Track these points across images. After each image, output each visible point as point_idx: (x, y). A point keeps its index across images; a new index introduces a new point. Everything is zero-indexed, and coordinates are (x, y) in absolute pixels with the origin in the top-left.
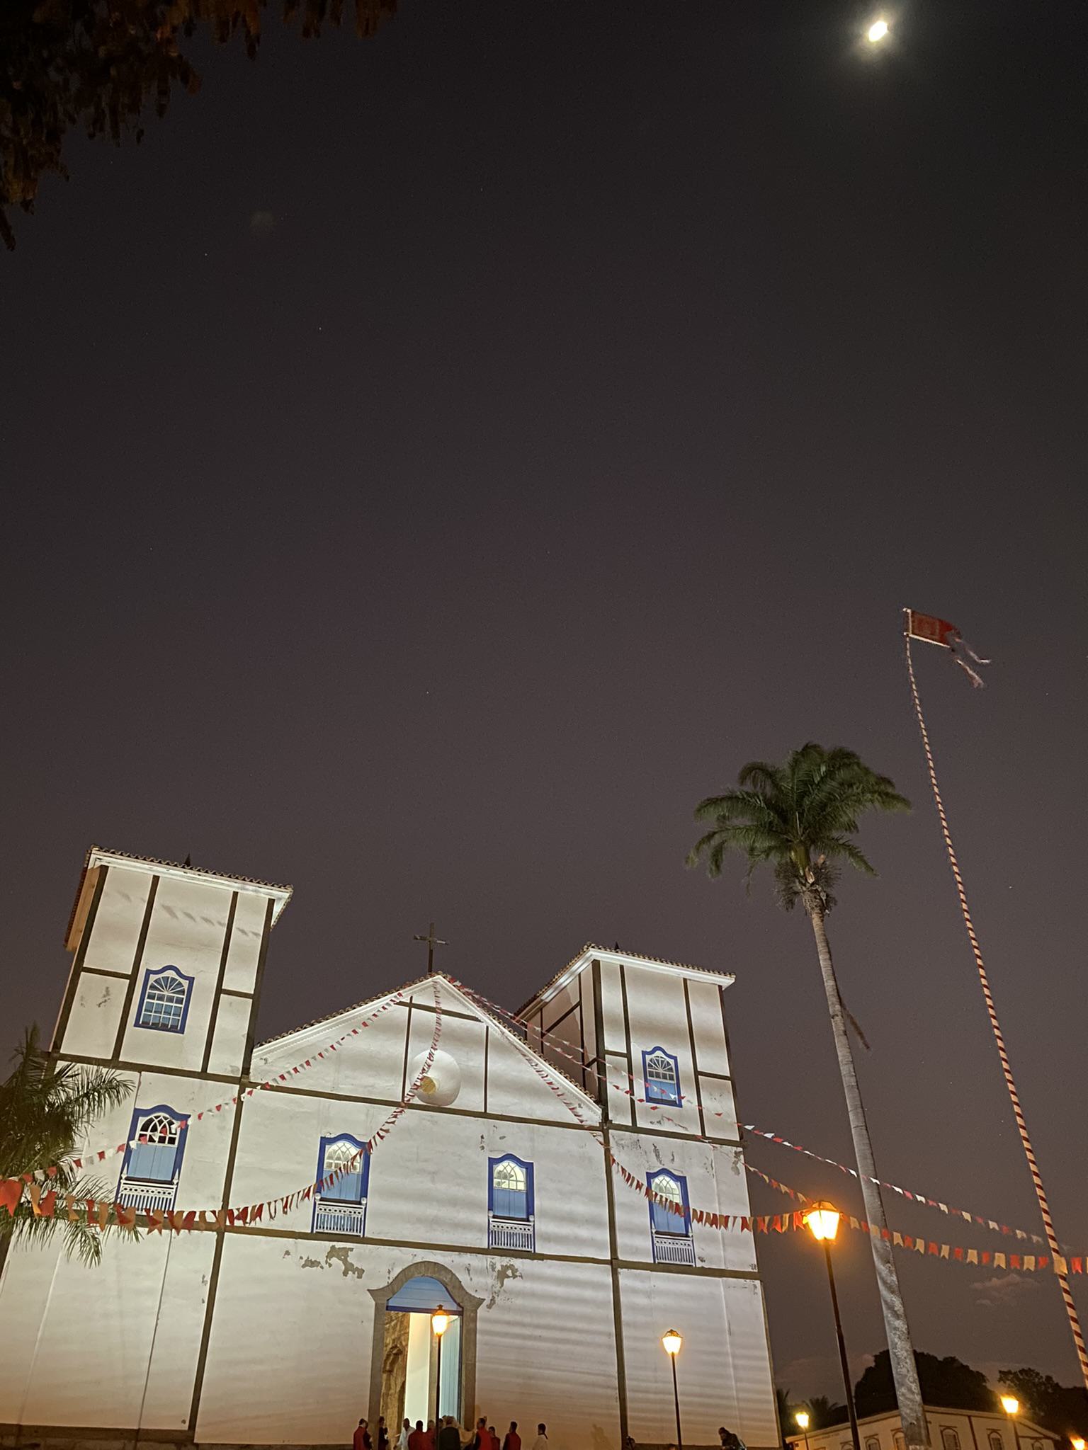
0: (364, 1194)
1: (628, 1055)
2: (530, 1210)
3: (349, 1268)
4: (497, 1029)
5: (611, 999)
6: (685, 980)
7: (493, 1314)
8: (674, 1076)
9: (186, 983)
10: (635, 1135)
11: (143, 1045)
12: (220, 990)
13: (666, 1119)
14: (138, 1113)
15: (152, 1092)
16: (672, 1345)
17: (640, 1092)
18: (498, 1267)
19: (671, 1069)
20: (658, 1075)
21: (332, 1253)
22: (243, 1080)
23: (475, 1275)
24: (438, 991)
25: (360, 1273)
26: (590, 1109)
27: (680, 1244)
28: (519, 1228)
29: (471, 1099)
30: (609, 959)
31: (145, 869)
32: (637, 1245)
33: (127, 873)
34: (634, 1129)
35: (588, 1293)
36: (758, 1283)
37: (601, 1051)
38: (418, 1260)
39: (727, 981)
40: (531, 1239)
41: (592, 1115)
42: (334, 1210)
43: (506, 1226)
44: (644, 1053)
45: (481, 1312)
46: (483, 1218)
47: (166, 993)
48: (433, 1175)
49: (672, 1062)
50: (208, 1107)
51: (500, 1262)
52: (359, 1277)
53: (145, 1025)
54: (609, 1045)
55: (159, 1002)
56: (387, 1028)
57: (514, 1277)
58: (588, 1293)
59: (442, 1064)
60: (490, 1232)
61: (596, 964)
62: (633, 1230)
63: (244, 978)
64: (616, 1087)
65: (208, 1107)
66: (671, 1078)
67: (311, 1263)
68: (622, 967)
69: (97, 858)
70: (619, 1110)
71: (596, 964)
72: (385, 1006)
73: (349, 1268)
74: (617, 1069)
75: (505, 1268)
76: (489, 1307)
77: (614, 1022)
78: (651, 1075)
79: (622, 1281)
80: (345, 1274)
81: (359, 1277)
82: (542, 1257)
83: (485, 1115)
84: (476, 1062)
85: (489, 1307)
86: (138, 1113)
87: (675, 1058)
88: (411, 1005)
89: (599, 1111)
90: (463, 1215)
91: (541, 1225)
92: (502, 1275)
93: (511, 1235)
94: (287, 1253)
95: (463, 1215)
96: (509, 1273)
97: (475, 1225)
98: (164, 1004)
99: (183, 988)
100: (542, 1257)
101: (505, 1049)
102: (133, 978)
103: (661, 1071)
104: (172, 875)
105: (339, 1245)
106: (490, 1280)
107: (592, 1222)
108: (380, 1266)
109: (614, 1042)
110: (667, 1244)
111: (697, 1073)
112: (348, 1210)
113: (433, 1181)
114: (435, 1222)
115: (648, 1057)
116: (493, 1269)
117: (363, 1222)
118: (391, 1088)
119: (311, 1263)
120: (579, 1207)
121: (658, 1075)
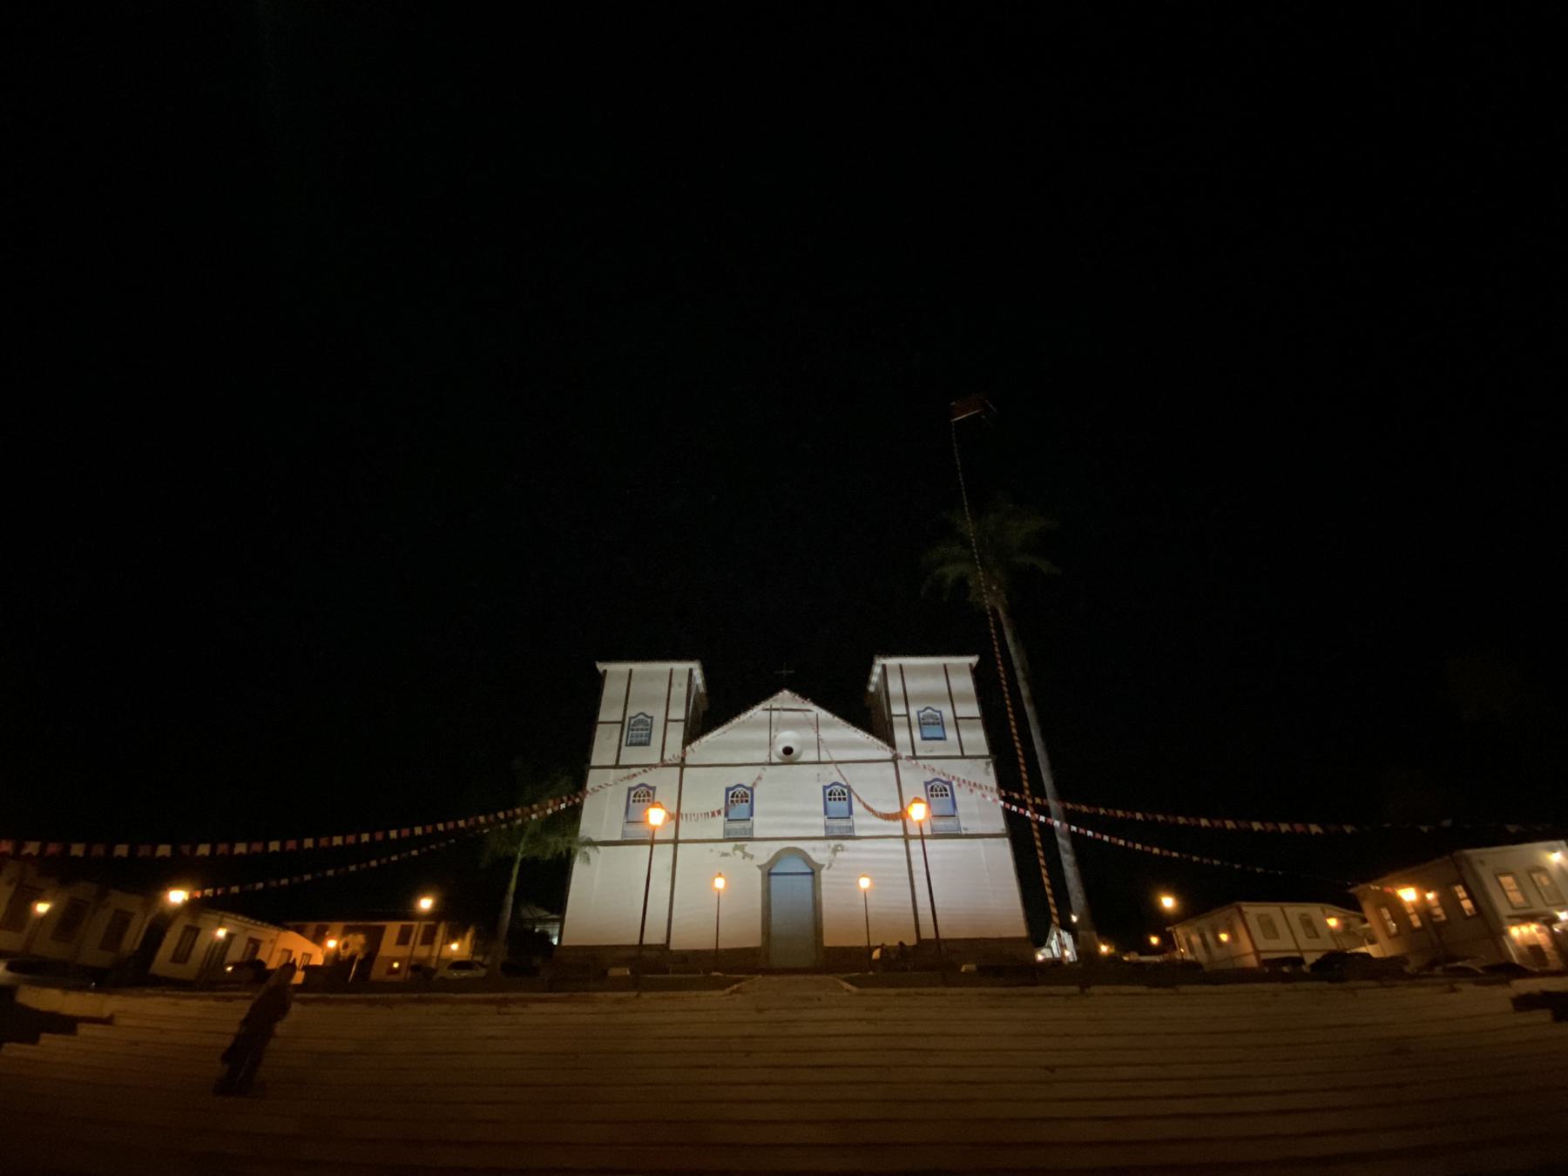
1: (908, 715)
2: (851, 812)
3: (745, 855)
4: (824, 715)
5: (895, 686)
7: (831, 872)
8: (941, 723)
11: (631, 755)
12: (667, 720)
13: (938, 748)
14: (630, 789)
16: (720, 883)
17: (917, 735)
21: (736, 848)
22: (682, 765)
23: (819, 852)
24: (785, 697)
25: (752, 857)
28: (844, 823)
29: (813, 756)
30: (892, 662)
31: (621, 668)
33: (615, 671)
34: (914, 757)
35: (891, 856)
37: (891, 716)
39: (974, 660)
40: (852, 828)
41: (887, 753)
42: (736, 825)
45: (824, 872)
46: (821, 820)
51: (833, 843)
53: (631, 744)
55: (637, 732)
56: (757, 725)
58: (891, 856)
59: (787, 737)
60: (826, 827)
61: (884, 667)
63: (679, 712)
64: (901, 735)
65: (664, 781)
69: (601, 667)
71: (884, 667)
72: (758, 712)
73: (745, 855)
74: (901, 724)
83: (819, 763)
84: (810, 735)
86: (630, 789)
88: (771, 710)
90: (808, 821)
92: (835, 851)
95: (808, 821)
97: (817, 824)
98: (641, 734)
99: (646, 723)
101: (828, 725)
102: (623, 723)
104: (638, 667)
106: (828, 854)
109: (897, 709)
112: (743, 824)
114: (792, 826)
117: (751, 829)
118: (762, 756)
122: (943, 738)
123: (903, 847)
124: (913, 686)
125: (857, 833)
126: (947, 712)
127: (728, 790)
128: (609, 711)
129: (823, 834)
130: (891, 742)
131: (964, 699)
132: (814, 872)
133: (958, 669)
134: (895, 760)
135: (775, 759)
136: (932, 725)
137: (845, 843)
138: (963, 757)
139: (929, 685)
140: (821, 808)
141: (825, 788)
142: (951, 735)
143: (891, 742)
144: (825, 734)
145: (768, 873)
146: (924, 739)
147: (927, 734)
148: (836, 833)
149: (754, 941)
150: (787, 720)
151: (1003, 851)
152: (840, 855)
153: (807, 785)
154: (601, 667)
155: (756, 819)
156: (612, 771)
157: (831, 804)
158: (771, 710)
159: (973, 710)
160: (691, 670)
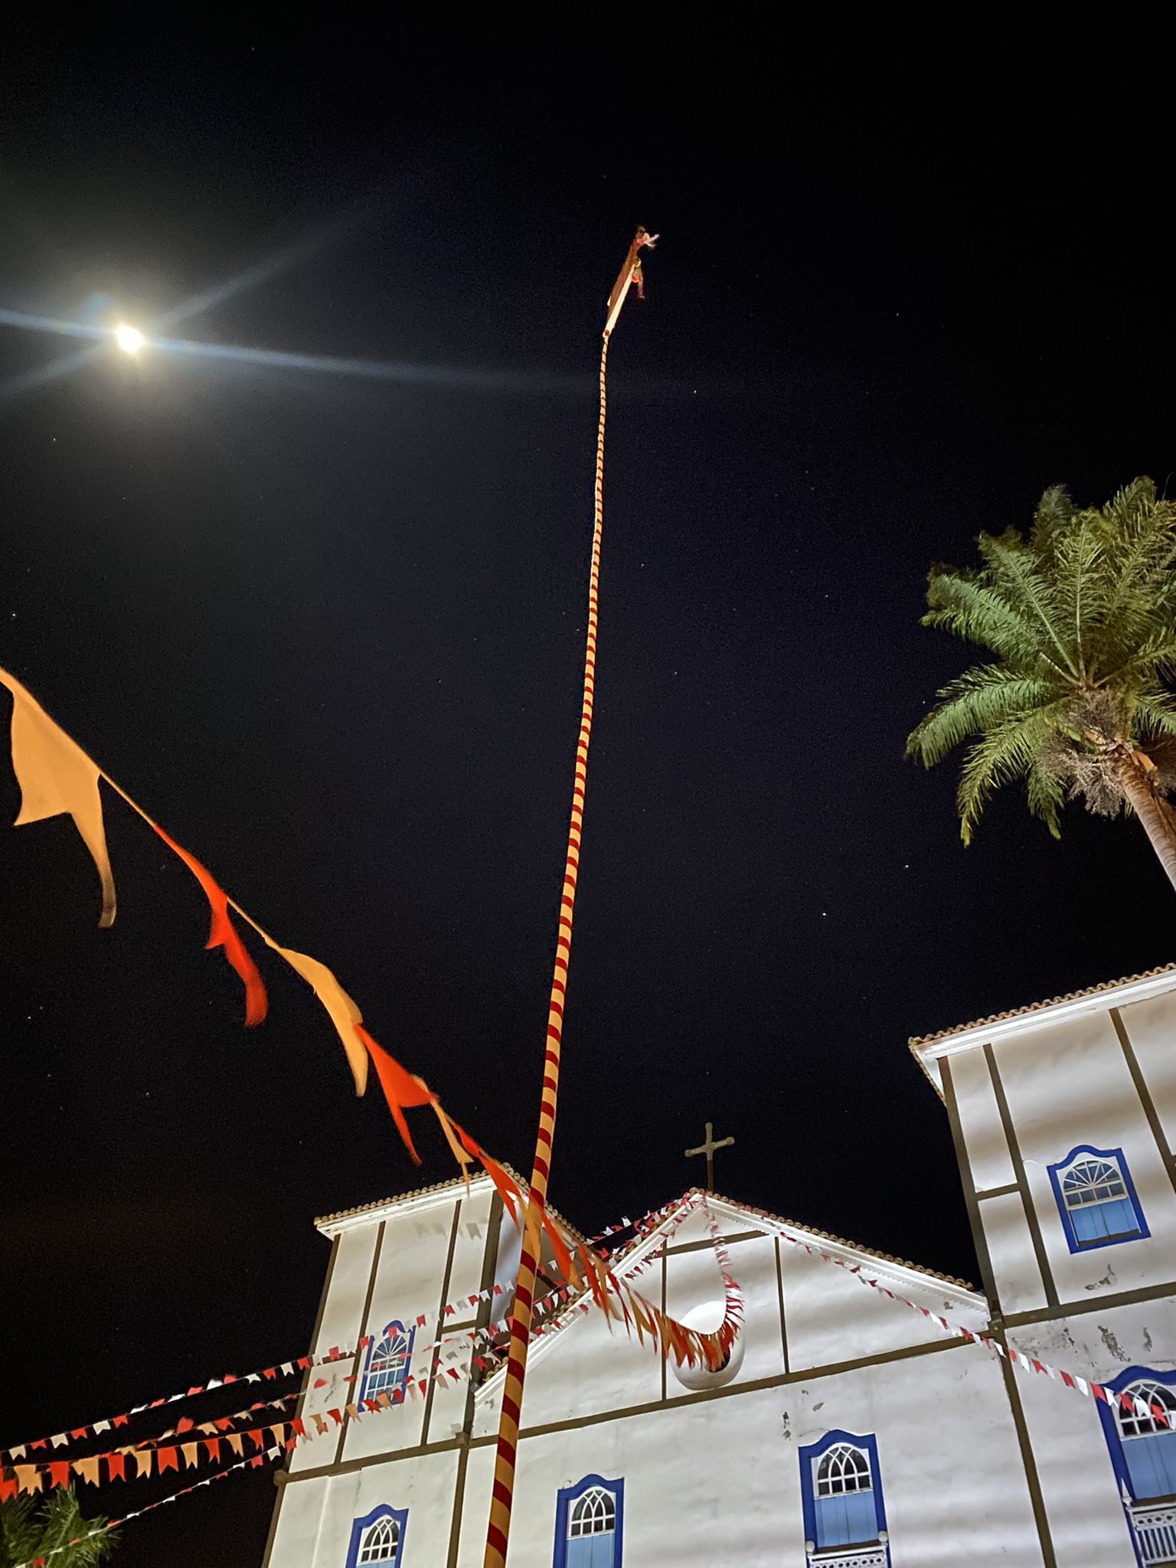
1: (1022, 1186)
2: (882, 1526)
10: (1058, 1324)
12: (441, 1330)
15: (376, 1488)
17: (1055, 1240)
19: (1114, 1175)
20: (1087, 1197)
24: (700, 1212)
26: (972, 1306)
34: (1056, 1310)
41: (973, 1312)
44: (1052, 1170)
47: (388, 1358)
48: (714, 1505)
49: (1112, 1161)
50: (423, 1490)
54: (982, 1181)
62: (1078, 1514)
64: (1006, 1252)
66: (1117, 1190)
68: (988, 1048)
69: (326, 1227)
70: (1019, 1288)
74: (1005, 1219)
77: (986, 1145)
78: (1073, 1200)
83: (788, 1378)
87: (1118, 1153)
89: (982, 1302)
101: (809, 1261)
103: (1092, 1186)
104: (393, 1212)
107: (994, 1517)
109: (987, 1176)
113: (715, 1515)
115: (1061, 1175)
120: (969, 1496)
121: (1087, 1197)
124: (1025, 1096)
128: (335, 1333)
134: (998, 1327)
140: (798, 1518)
141: (806, 1455)
144: (804, 1293)
147: (1086, 1234)
154: (326, 1227)
156: (329, 1480)
158: (664, 1253)
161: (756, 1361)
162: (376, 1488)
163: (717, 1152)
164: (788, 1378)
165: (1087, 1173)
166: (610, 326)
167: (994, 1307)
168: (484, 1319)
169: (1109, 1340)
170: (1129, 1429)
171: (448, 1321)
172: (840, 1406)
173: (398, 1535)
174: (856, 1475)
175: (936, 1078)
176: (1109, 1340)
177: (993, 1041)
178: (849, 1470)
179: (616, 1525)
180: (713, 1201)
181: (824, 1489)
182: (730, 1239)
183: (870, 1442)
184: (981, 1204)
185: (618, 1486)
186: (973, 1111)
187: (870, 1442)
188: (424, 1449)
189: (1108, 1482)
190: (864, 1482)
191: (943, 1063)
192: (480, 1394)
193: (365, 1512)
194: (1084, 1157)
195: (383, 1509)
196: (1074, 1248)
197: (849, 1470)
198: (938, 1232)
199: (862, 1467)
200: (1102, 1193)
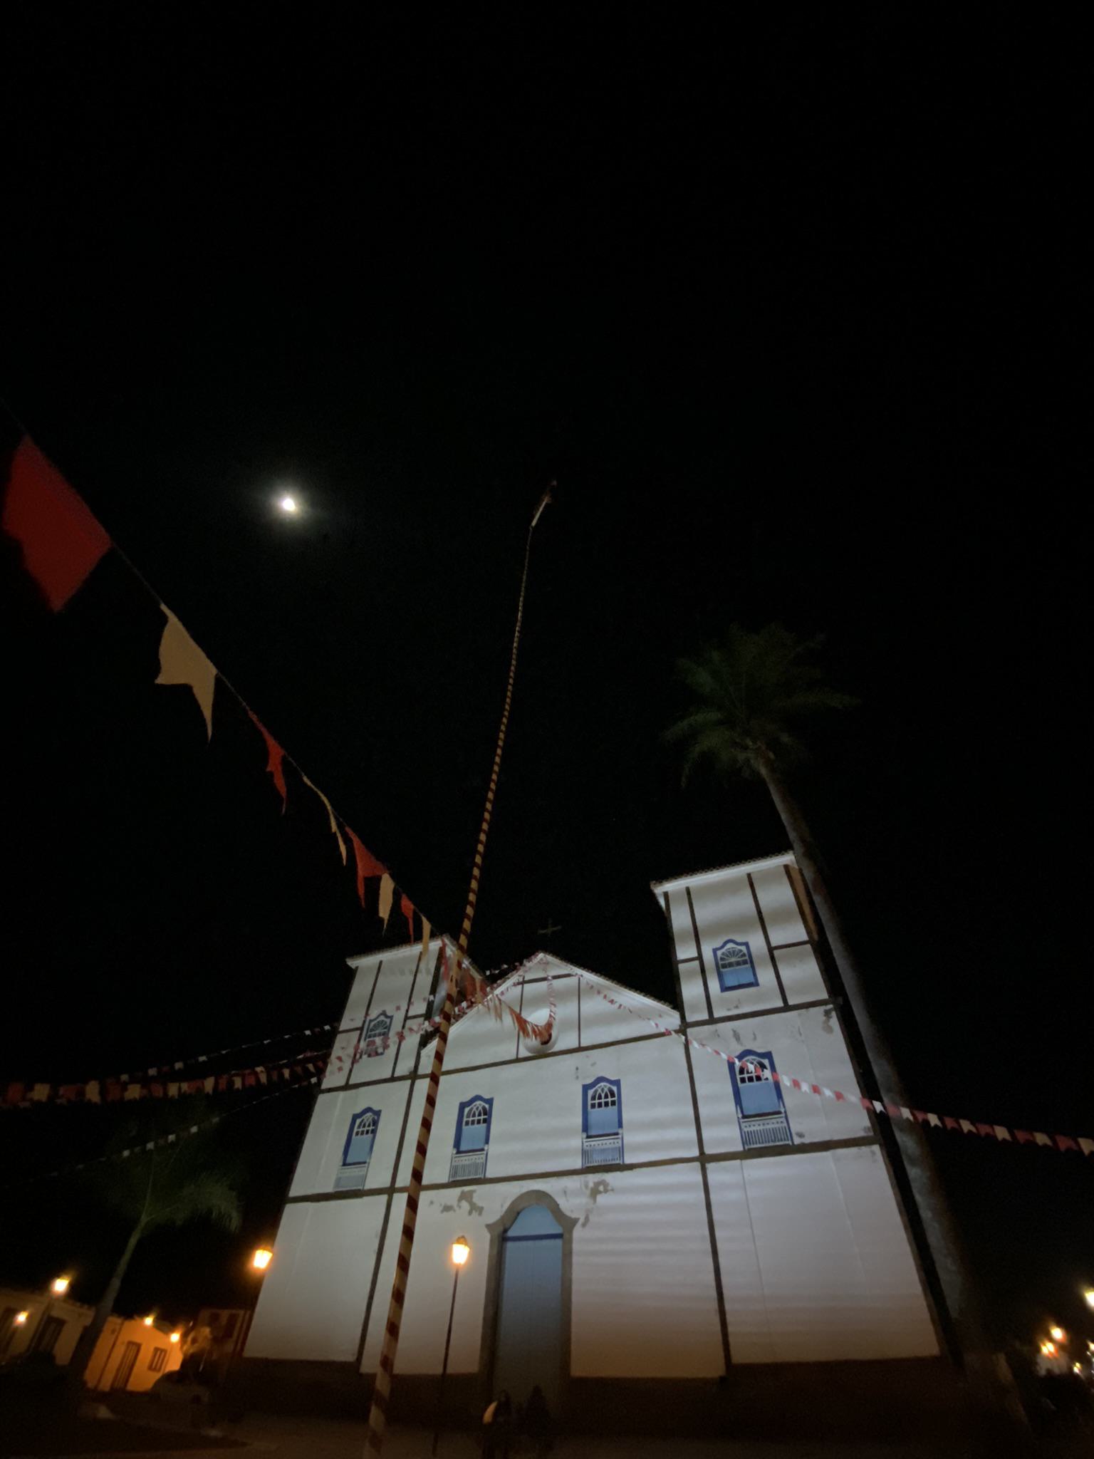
0: (487, 1142)
1: (700, 957)
2: (620, 1125)
6: (749, 875)
9: (388, 1021)
12: (407, 1018)
13: (746, 1001)
17: (714, 985)
18: (591, 1185)
20: (731, 965)
21: (463, 1196)
23: (570, 1196)
24: (542, 964)
25: (480, 1210)
27: (773, 1124)
30: (673, 886)
32: (724, 1133)
34: (712, 1020)
36: (876, 1148)
38: (524, 1190)
41: (671, 1020)
43: (596, 1143)
44: (715, 951)
45: (578, 1233)
46: (577, 1141)
49: (743, 948)
50: (390, 1101)
51: (592, 1179)
52: (480, 1214)
57: (606, 1191)
60: (585, 1153)
61: (666, 895)
62: (718, 1121)
64: (691, 990)
66: (745, 962)
67: (447, 1208)
68: (688, 890)
69: (352, 963)
74: (690, 974)
75: (597, 1184)
76: (584, 1225)
78: (724, 966)
79: (711, 1178)
80: (470, 1213)
81: (480, 1214)
82: (631, 1167)
83: (580, 1049)
85: (584, 1225)
87: (746, 944)
91: (629, 1137)
92: (595, 1193)
93: (603, 1151)
94: (432, 1203)
96: (601, 1188)
100: (631, 1167)
103: (733, 960)
104: (386, 956)
105: (467, 1189)
106: (584, 1200)
108: (496, 1200)
109: (684, 951)
110: (756, 1126)
111: (771, 950)
115: (719, 953)
116: (587, 1186)
119: (447, 1208)
121: (731, 965)
122: (755, 984)
123: (700, 1178)
124: (705, 913)
125: (629, 1160)
126: (757, 942)
127: (586, 1088)
128: (352, 1018)
129: (577, 1164)
130: (675, 1001)
131: (782, 916)
132: (564, 1230)
133: (768, 876)
134: (684, 1027)
135: (524, 1053)
136: (735, 968)
137: (610, 1177)
138: (787, 1008)
139: (734, 906)
140: (579, 1121)
142: (766, 976)
143: (675, 1001)
144: (592, 1006)
145: (502, 1237)
146: (724, 989)
147: (730, 982)
148: (597, 1160)
149: (466, 1358)
150: (558, 993)
151: (870, 1167)
152: (600, 1198)
153: (562, 1081)
154: (352, 963)
155: (492, 1148)
157: (595, 1114)
158: (523, 983)
159: (797, 932)
160: (442, 951)
161: (564, 1040)
162: (364, 1099)
163: (553, 932)
164: (580, 1049)
165: (732, 953)
166: (534, 523)
167: (683, 1017)
168: (428, 1016)
169: (737, 1036)
170: (743, 1080)
171: (410, 1014)
172: (604, 1065)
173: (375, 1123)
174: (610, 1100)
175: (662, 902)
176: (737, 1036)
177: (690, 885)
178: (606, 1097)
179: (487, 1121)
180: (550, 958)
181: (593, 1106)
182: (555, 977)
183: (617, 1083)
184: (681, 967)
185: (490, 1102)
186: (680, 920)
187: (617, 1083)
188: (393, 1079)
189: (731, 1106)
190: (613, 1103)
191: (666, 895)
192: (424, 1052)
193: (358, 1111)
194: (730, 945)
195: (369, 1110)
196: (724, 989)
197: (606, 1097)
198: (659, 980)
199: (613, 1095)
200: (738, 964)
